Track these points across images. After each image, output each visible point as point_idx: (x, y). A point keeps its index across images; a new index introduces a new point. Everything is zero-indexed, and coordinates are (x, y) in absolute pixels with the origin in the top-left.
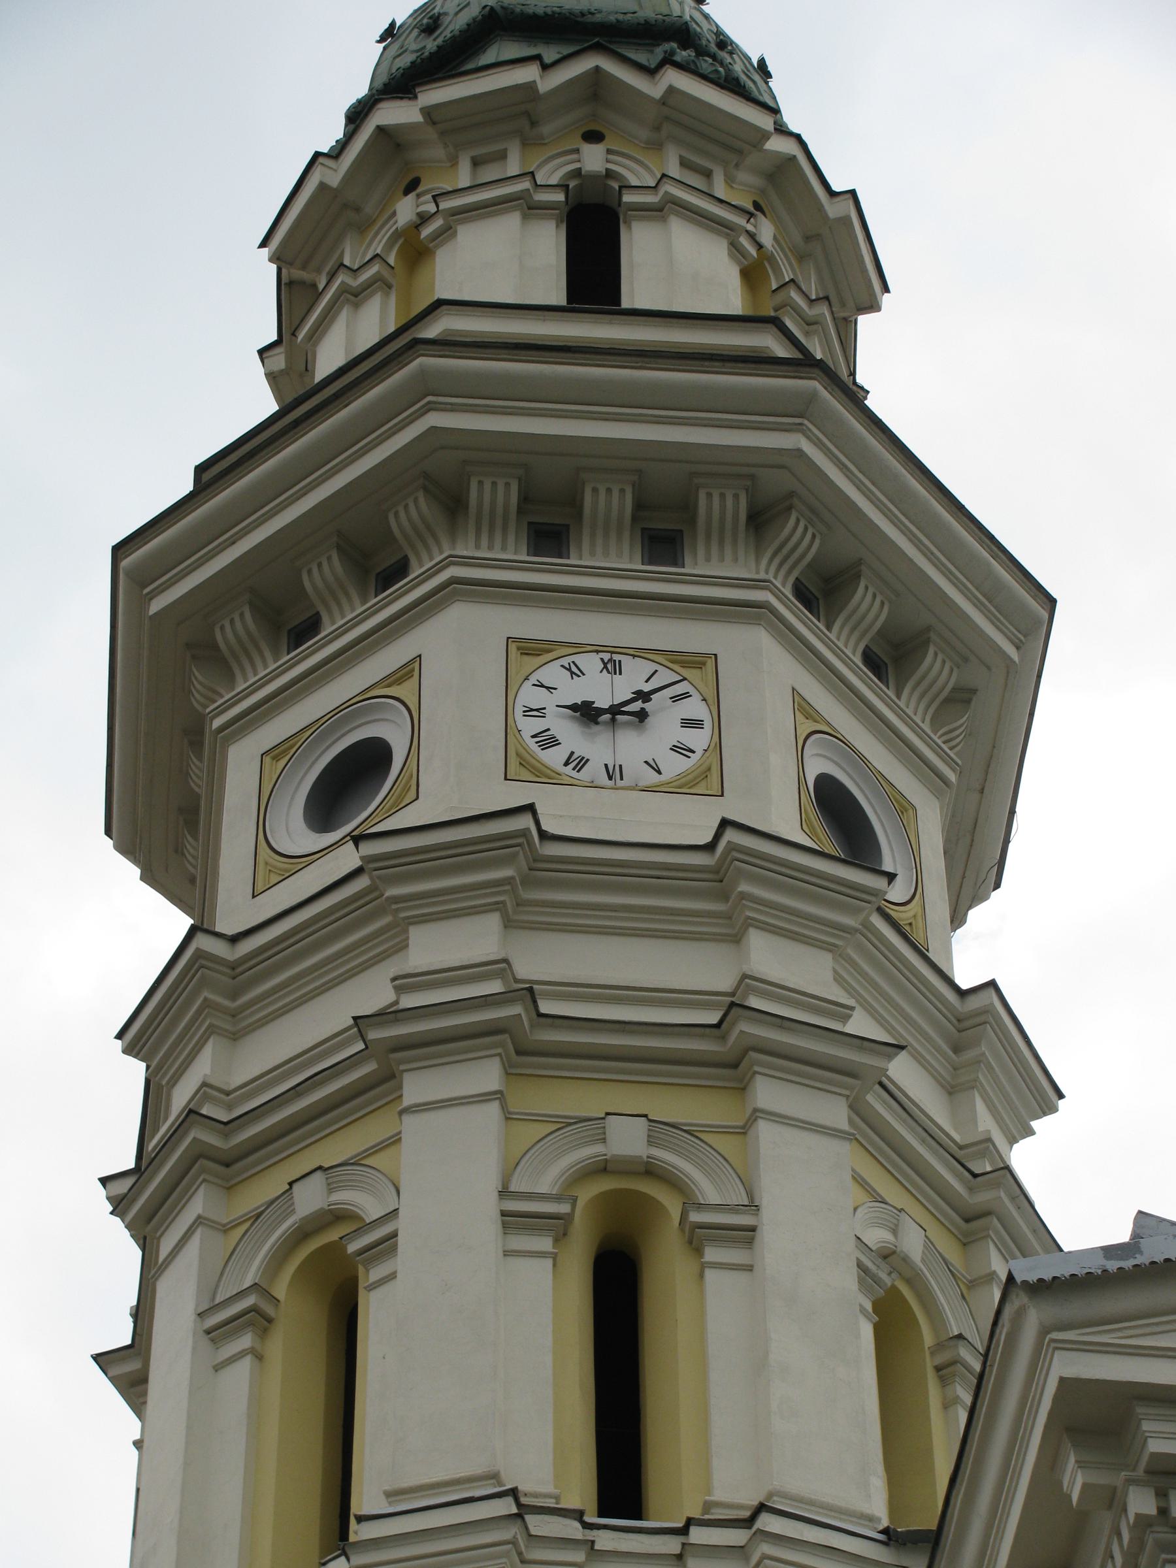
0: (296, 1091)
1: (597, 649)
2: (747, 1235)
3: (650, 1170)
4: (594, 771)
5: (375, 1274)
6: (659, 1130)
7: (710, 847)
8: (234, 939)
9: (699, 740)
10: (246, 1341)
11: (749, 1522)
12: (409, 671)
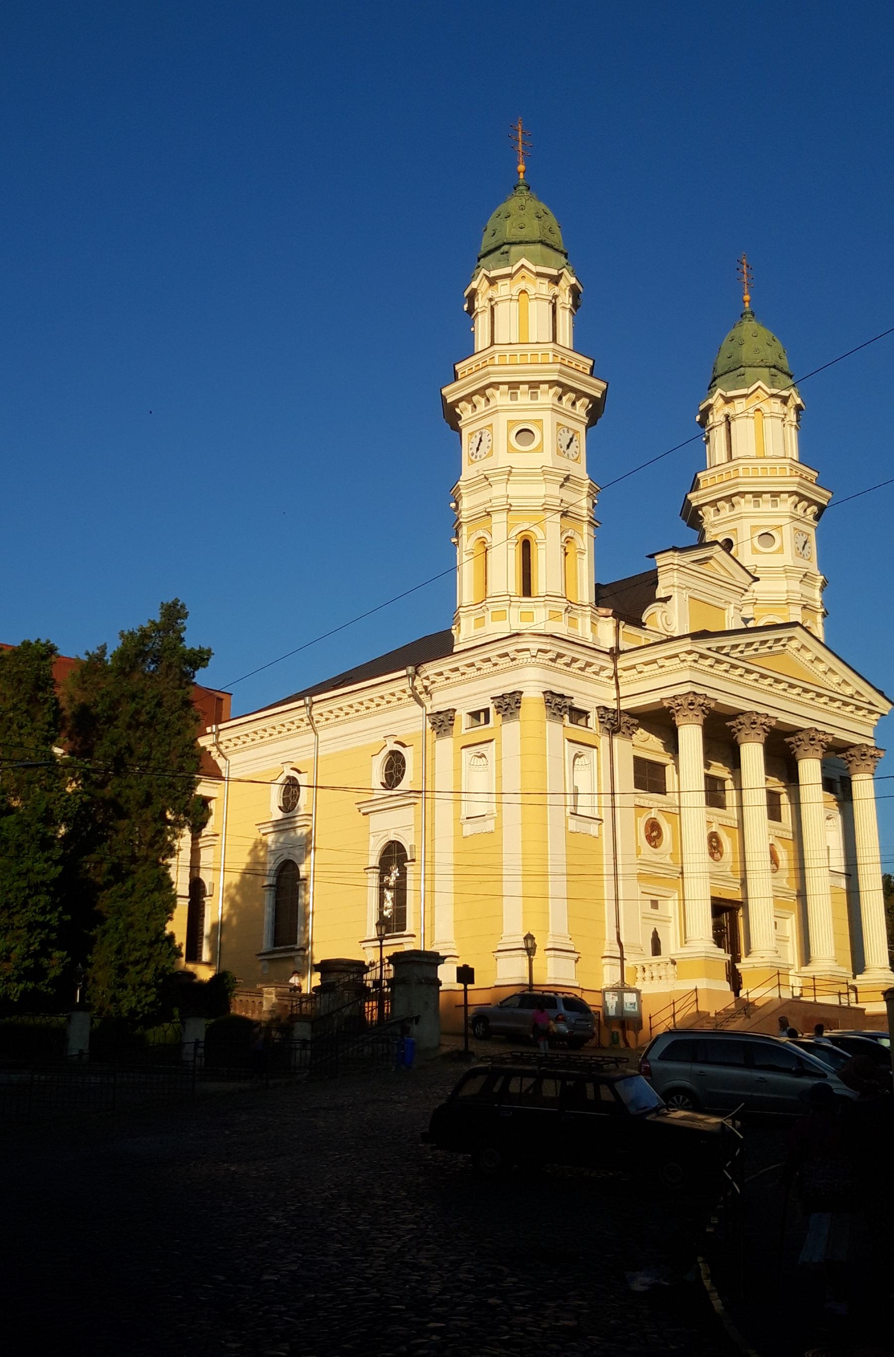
1: (567, 427)
10: (513, 546)
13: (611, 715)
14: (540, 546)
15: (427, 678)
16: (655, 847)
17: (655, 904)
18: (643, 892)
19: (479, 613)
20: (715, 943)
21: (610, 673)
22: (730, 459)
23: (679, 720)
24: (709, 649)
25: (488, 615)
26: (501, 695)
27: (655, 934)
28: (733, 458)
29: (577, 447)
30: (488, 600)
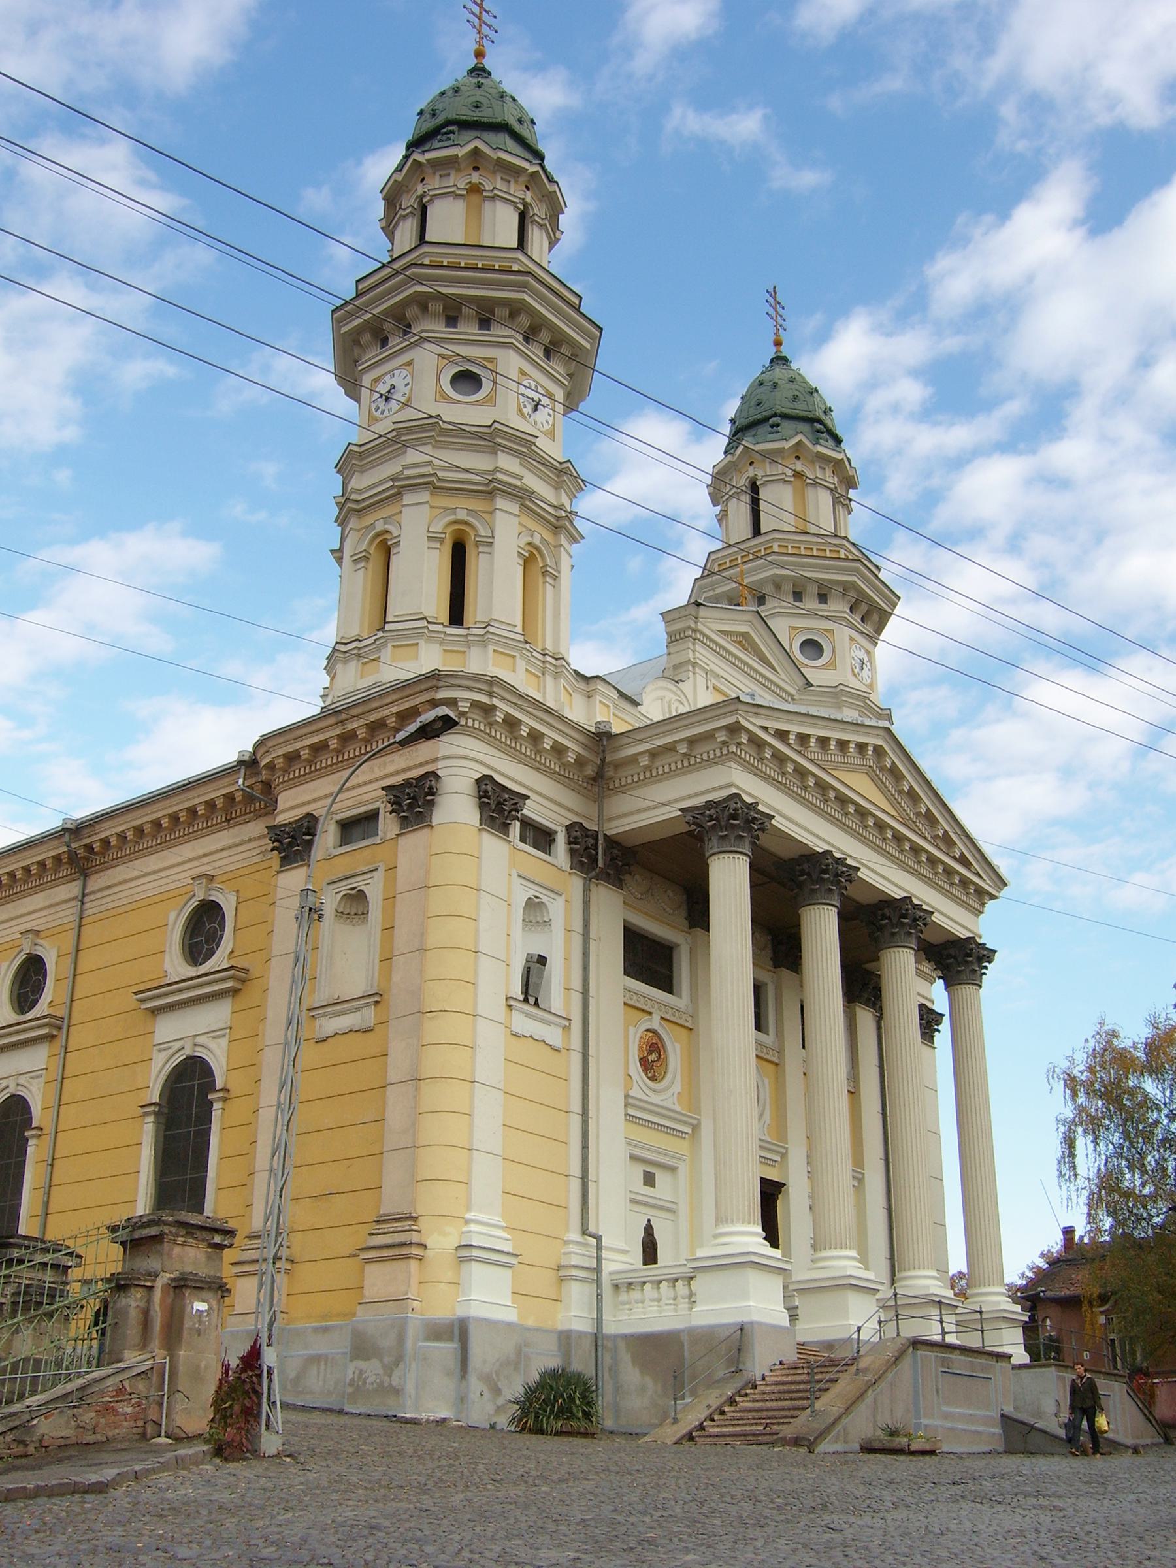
0: (462, 482)
2: (555, 578)
3: (537, 548)
4: (531, 420)
5: (481, 549)
6: (543, 539)
7: (561, 463)
8: (443, 422)
9: (551, 420)
10: (438, 545)
11: (556, 659)
12: (491, 360)
13: (591, 841)
14: (481, 549)
15: (271, 767)
16: (653, 1079)
17: (649, 1180)
18: (633, 1158)
19: (372, 652)
20: (765, 1239)
21: (590, 771)
22: (757, 531)
23: (713, 844)
24: (765, 729)
25: (387, 654)
26: (398, 780)
27: (649, 1230)
28: (762, 532)
29: (549, 415)
30: (388, 627)
